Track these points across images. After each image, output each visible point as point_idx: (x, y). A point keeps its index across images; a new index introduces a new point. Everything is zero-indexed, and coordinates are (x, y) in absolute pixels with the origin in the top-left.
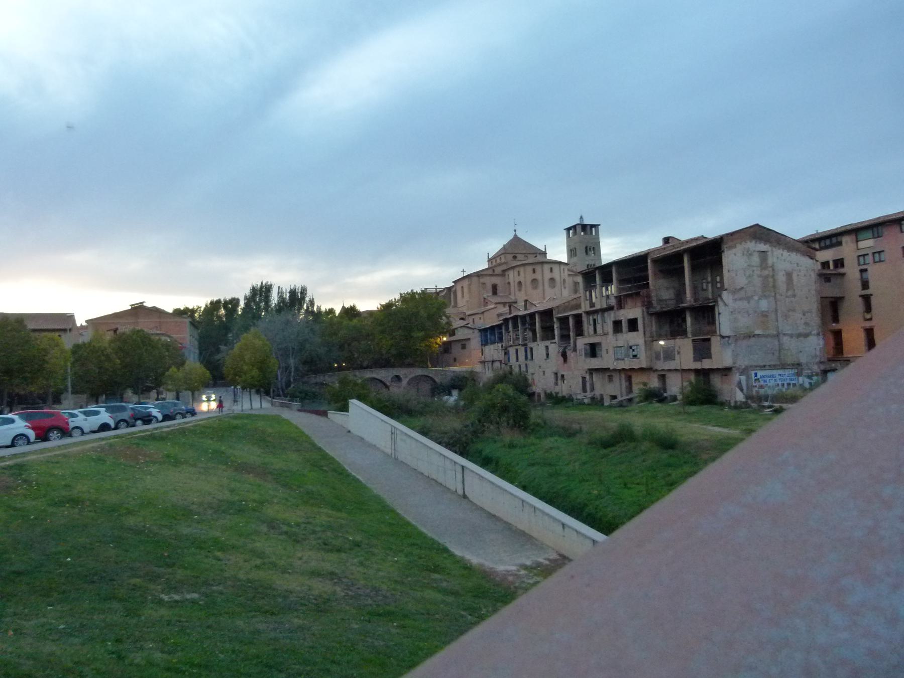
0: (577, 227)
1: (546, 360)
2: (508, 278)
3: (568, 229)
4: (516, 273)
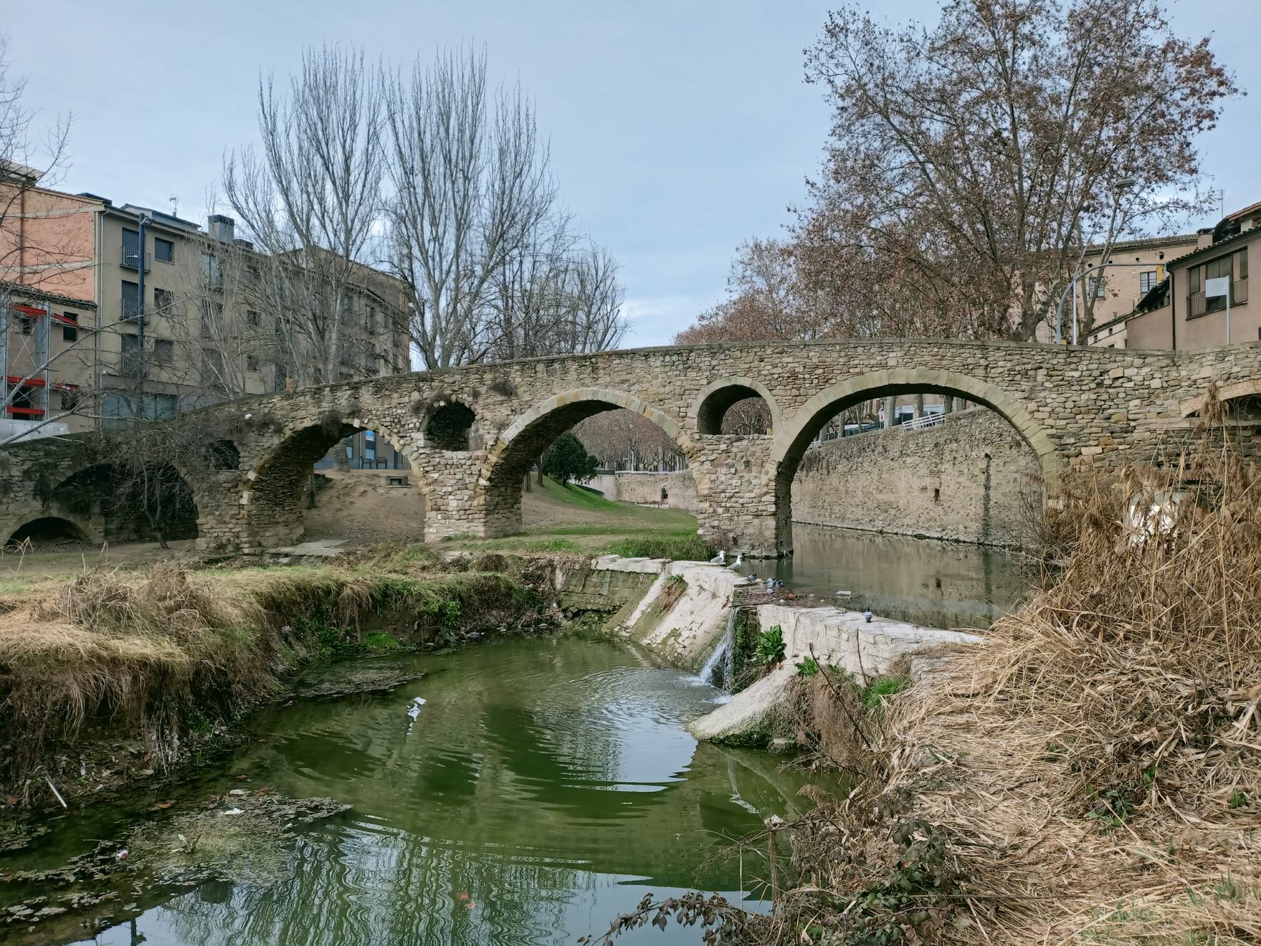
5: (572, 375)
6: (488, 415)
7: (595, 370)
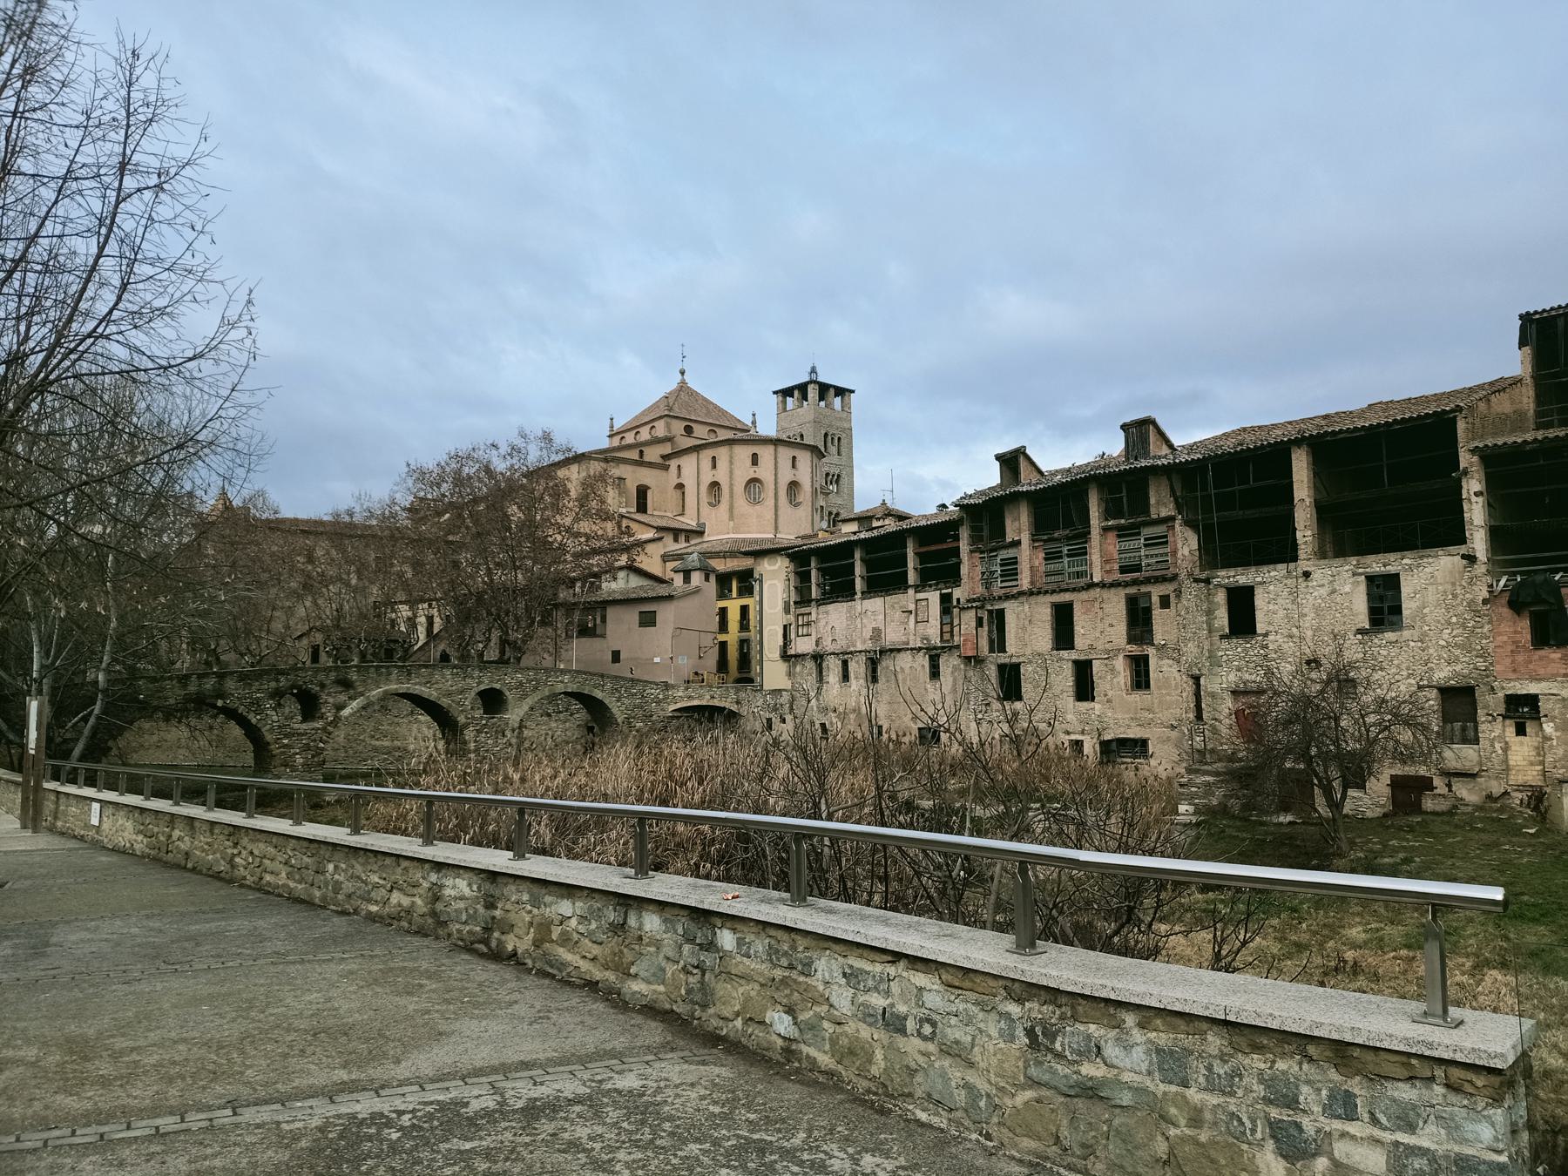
0: (810, 388)
1: (1361, 631)
2: (679, 475)
3: (786, 393)
4: (706, 463)
5: (394, 676)
6: (331, 700)
7: (409, 674)
